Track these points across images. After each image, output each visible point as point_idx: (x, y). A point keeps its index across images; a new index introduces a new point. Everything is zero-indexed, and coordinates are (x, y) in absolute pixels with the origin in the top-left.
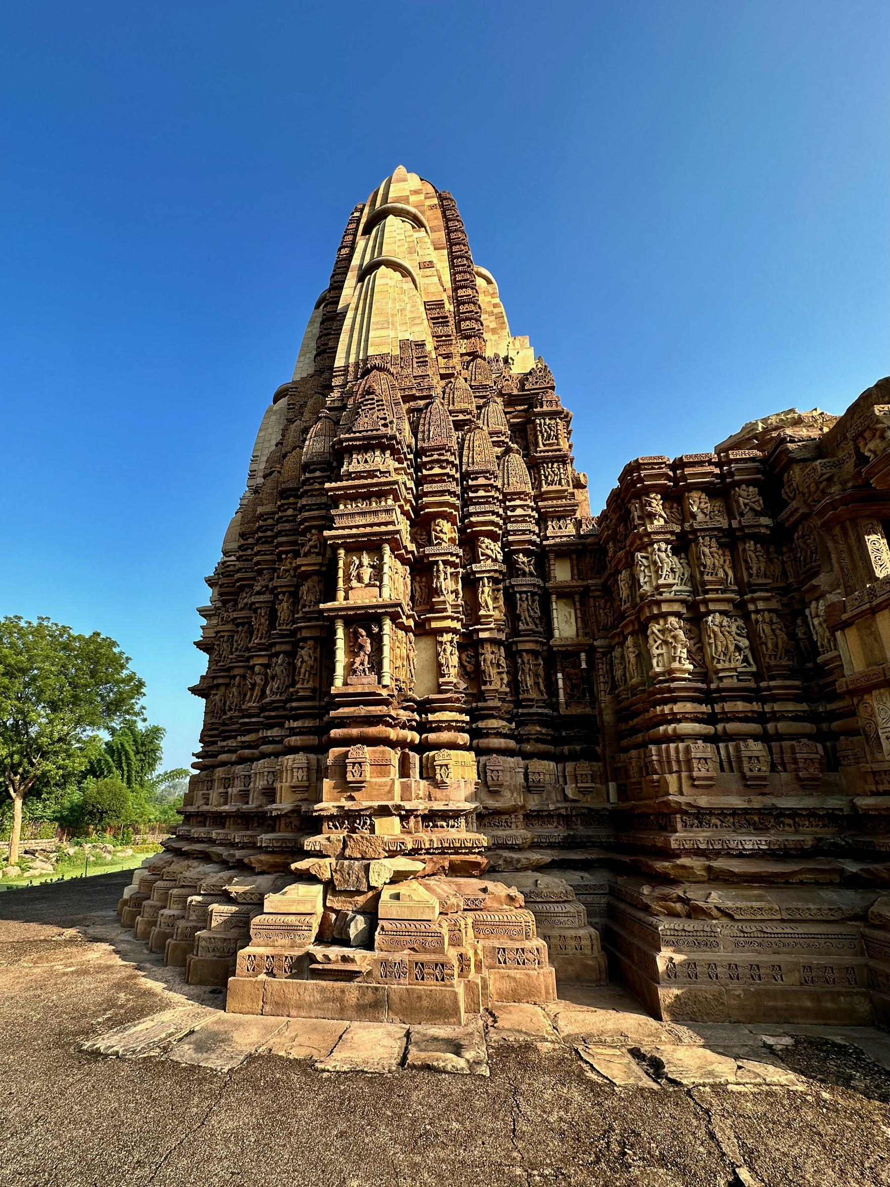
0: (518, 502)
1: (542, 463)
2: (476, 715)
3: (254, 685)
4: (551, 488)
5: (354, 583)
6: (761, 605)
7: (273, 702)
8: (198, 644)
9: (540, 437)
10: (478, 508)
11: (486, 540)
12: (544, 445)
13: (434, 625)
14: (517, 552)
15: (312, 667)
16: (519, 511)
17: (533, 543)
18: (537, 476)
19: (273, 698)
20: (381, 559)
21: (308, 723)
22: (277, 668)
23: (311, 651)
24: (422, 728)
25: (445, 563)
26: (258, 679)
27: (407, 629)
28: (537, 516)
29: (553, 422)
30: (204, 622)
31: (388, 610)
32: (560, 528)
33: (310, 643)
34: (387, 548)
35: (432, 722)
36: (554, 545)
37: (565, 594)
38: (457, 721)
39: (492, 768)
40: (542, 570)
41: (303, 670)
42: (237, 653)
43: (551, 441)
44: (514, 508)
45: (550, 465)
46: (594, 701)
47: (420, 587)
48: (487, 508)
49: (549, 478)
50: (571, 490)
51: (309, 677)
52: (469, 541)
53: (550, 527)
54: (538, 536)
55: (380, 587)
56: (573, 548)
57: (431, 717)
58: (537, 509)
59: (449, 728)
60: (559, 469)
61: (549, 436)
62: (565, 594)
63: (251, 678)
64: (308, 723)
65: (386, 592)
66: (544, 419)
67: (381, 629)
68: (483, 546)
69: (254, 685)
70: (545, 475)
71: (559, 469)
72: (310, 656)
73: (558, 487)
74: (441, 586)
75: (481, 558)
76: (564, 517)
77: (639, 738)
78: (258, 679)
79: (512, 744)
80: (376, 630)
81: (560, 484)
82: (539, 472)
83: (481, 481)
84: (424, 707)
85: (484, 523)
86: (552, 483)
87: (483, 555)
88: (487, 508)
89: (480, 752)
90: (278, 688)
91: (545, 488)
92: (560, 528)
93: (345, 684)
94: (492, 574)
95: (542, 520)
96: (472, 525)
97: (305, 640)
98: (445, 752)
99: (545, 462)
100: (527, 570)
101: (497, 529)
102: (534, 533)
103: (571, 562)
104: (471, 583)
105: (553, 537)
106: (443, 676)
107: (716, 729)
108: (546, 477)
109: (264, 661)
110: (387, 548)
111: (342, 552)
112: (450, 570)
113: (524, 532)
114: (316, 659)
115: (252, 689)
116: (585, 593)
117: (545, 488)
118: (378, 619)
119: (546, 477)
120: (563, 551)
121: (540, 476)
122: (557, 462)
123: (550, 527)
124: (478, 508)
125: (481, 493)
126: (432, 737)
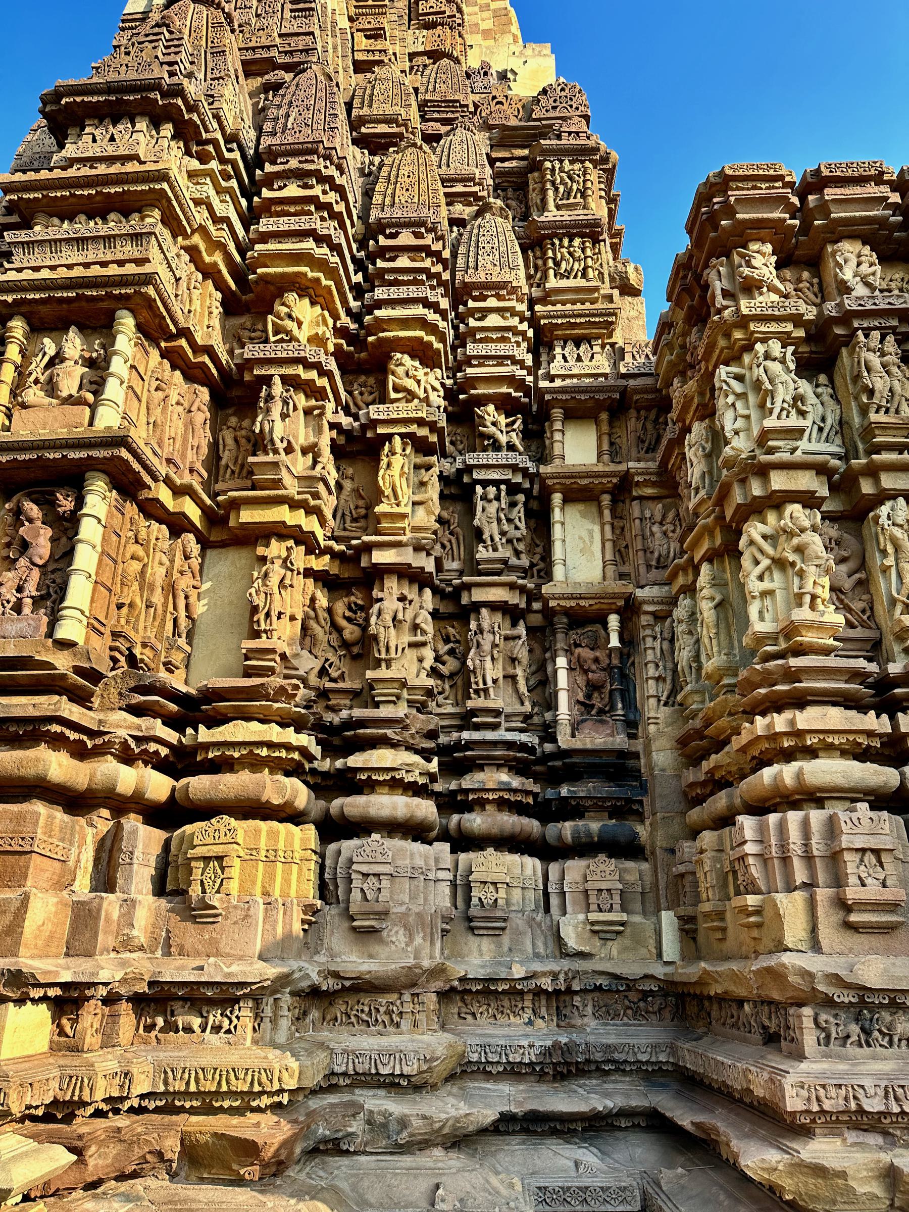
0: (492, 302)
1: (551, 237)
2: (340, 739)
5: (34, 395)
9: (551, 193)
10: (395, 293)
11: (406, 359)
12: (558, 207)
13: (247, 516)
14: (481, 401)
16: (493, 320)
17: (519, 384)
18: (540, 262)
24: (180, 762)
27: (177, 525)
28: (530, 333)
29: (577, 166)
31: (95, 453)
32: (579, 359)
34: (127, 322)
35: (207, 746)
36: (563, 390)
37: (580, 492)
38: (270, 745)
39: (364, 869)
40: (536, 436)
43: (572, 200)
44: (484, 313)
45: (566, 242)
46: (632, 726)
47: (236, 440)
48: (413, 292)
49: (564, 265)
50: (606, 289)
52: (365, 361)
53: (559, 358)
54: (533, 370)
55: (93, 408)
56: (601, 396)
58: (533, 321)
59: (255, 764)
60: (583, 250)
61: (568, 193)
62: (580, 492)
66: (561, 162)
67: (80, 502)
68: (400, 370)
70: (554, 259)
71: (583, 250)
73: (580, 282)
74: (271, 430)
75: (393, 395)
76: (588, 339)
77: (720, 801)
79: (425, 809)
80: (66, 504)
81: (584, 276)
82: (544, 253)
83: (406, 238)
84: (193, 709)
85: (404, 323)
86: (567, 275)
87: (396, 389)
88: (413, 292)
89: (333, 829)
91: (553, 282)
92: (579, 359)
94: (413, 428)
95: (542, 342)
99: (555, 235)
100: (503, 439)
101: (432, 338)
102: (521, 363)
103: (598, 430)
105: (563, 377)
106: (256, 635)
107: (902, 774)
108: (557, 264)
110: (127, 322)
112: (301, 400)
113: (500, 360)
116: (622, 489)
117: (553, 282)
118: (74, 479)
119: (557, 264)
120: (583, 406)
121: (545, 264)
122: (582, 235)
123: (559, 358)
124: (395, 293)
125: (404, 262)
126: (200, 785)
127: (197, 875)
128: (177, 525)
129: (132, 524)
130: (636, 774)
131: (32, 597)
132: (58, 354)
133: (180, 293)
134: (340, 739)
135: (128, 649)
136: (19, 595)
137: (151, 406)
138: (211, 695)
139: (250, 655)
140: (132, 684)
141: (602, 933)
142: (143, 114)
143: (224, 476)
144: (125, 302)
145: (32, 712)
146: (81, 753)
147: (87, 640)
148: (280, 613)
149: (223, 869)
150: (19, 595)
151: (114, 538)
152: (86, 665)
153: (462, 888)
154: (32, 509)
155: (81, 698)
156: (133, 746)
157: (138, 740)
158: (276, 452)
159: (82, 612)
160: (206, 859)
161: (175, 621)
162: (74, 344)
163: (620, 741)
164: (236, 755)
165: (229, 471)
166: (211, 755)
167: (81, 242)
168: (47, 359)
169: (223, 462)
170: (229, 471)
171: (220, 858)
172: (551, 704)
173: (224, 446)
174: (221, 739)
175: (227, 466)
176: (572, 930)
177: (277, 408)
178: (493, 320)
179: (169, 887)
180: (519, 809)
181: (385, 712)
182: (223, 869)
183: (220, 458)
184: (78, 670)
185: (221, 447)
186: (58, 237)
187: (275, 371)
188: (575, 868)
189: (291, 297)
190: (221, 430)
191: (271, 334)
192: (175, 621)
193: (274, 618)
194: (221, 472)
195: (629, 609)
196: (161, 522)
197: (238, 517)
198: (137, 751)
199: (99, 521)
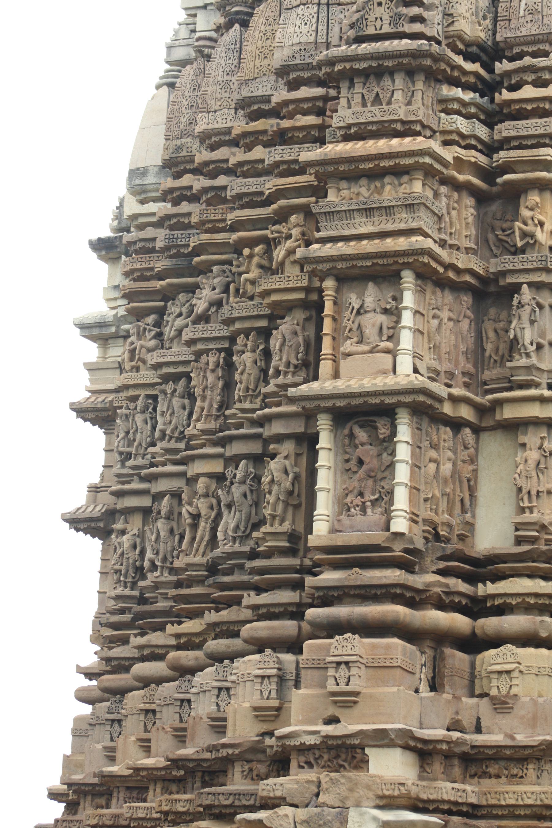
3: (196, 517)
7: (231, 555)
8: (83, 412)
13: (509, 413)
15: (290, 493)
19: (228, 548)
20: (397, 299)
21: (286, 596)
22: (233, 488)
23: (287, 462)
24: (476, 608)
25: (537, 286)
26: (202, 505)
33: (288, 447)
35: (493, 596)
38: (537, 595)
41: (271, 499)
42: (164, 444)
47: (496, 331)
51: (285, 511)
55: (393, 353)
57: (491, 588)
59: (528, 609)
63: (190, 504)
64: (286, 596)
65: (405, 364)
67: (394, 433)
69: (196, 517)
72: (286, 472)
74: (523, 337)
78: (202, 505)
90: (237, 527)
93: (333, 531)
97: (279, 439)
98: (508, 649)
106: (522, 510)
109: (217, 467)
111: (329, 284)
114: (297, 477)
115: (194, 526)
118: (388, 412)
126: (491, 624)
127: (494, 683)
128: (456, 425)
129: (427, 436)
131: (371, 501)
132: (362, 306)
133: (443, 225)
135: (434, 529)
136: (362, 500)
137: (432, 335)
138: (493, 559)
139: (518, 527)
140: (439, 554)
142: (399, 70)
143: (489, 365)
144: (407, 266)
145: (385, 581)
146: (412, 604)
147: (410, 529)
148: (538, 492)
149: (511, 679)
150: (362, 500)
151: (418, 450)
152: (411, 547)
154: (362, 435)
155: (407, 566)
156: (444, 598)
157: (447, 593)
158: (528, 355)
159: (406, 511)
160: (500, 673)
161: (462, 501)
162: (371, 296)
164: (514, 603)
165: (492, 360)
166: (496, 603)
167: (368, 211)
168: (355, 311)
169: (487, 354)
170: (492, 360)
171: (508, 672)
173: (487, 338)
174: (502, 591)
175: (490, 356)
177: (526, 313)
179: (477, 692)
182: (511, 679)
183: (484, 350)
184: (406, 551)
185: (484, 338)
186: (351, 208)
187: (521, 278)
189: (534, 198)
190: (483, 321)
191: (518, 239)
192: (462, 501)
193: (534, 498)
194: (486, 363)
196: (446, 425)
197: (502, 413)
198: (447, 601)
199: (408, 443)
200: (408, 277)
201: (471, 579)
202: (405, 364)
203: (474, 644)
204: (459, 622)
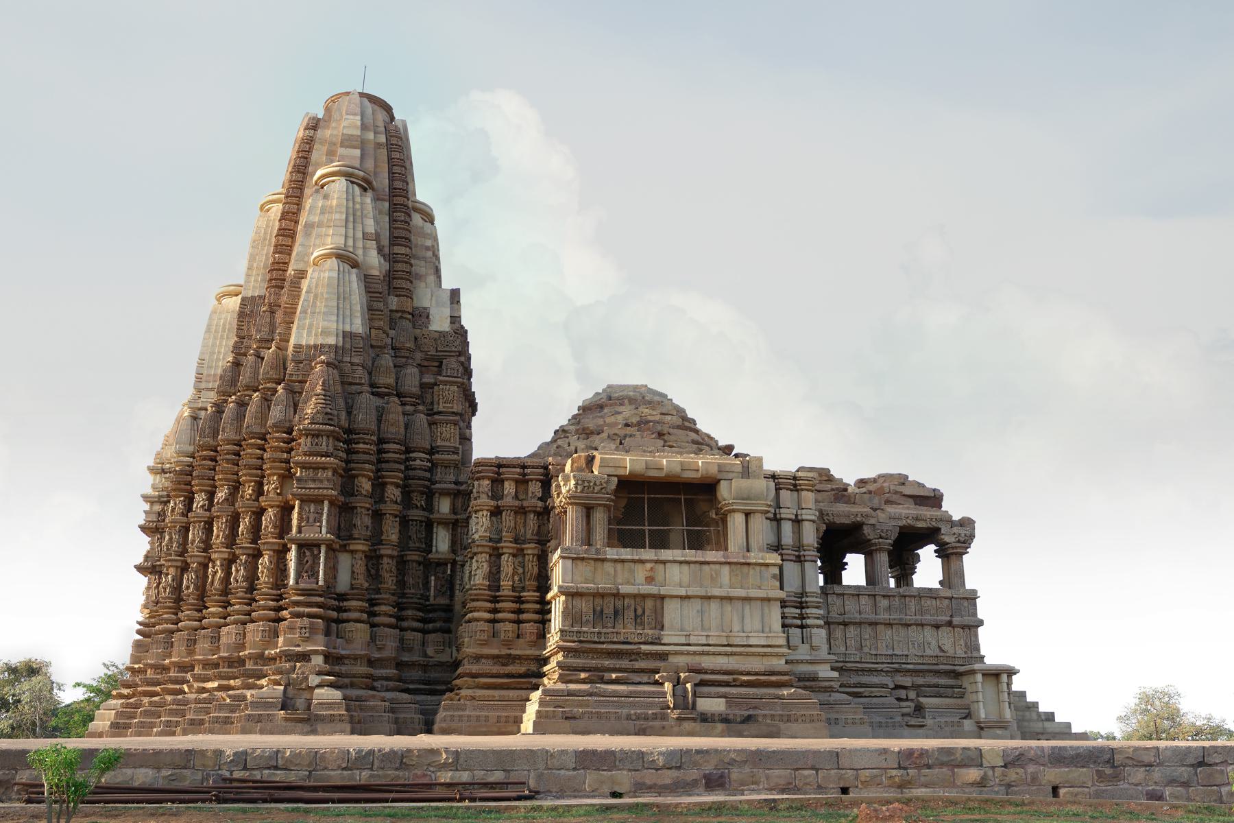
2: (373, 603)
4: (443, 443)
6: (529, 552)
13: (352, 547)
16: (418, 462)
24: (339, 610)
30: (147, 507)
37: (444, 523)
44: (415, 460)
46: (452, 597)
57: (345, 603)
59: (356, 610)
62: (444, 523)
79: (393, 620)
89: (373, 626)
91: (439, 443)
96: (383, 477)
104: (377, 516)
118: (318, 546)
130: (451, 611)
134: (373, 603)
141: (437, 652)
153: (402, 640)
154: (308, 553)
163: (447, 602)
167: (314, 481)
172: (429, 590)
176: (430, 651)
178: (418, 462)
180: (418, 621)
181: (383, 596)
188: (432, 637)
195: (454, 563)
200: (326, 503)
201: (339, 600)
202: (324, 530)
203: (339, 621)
204: (334, 614)
